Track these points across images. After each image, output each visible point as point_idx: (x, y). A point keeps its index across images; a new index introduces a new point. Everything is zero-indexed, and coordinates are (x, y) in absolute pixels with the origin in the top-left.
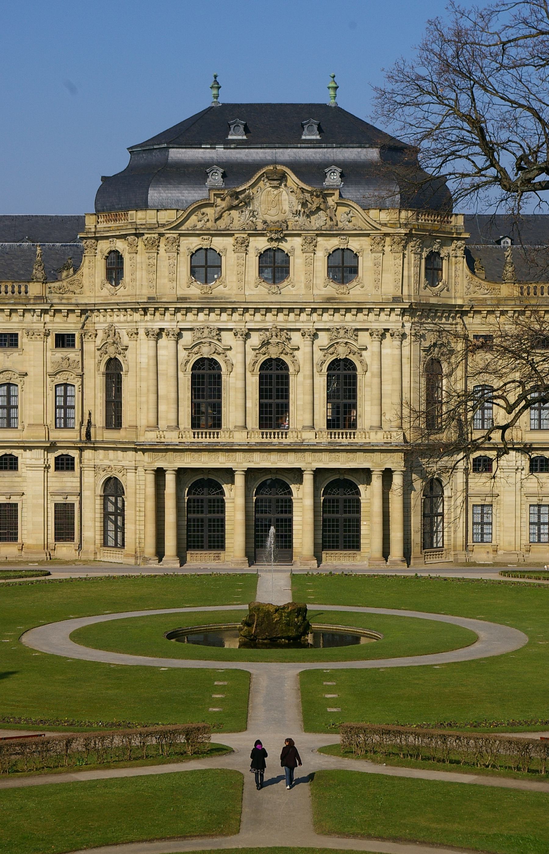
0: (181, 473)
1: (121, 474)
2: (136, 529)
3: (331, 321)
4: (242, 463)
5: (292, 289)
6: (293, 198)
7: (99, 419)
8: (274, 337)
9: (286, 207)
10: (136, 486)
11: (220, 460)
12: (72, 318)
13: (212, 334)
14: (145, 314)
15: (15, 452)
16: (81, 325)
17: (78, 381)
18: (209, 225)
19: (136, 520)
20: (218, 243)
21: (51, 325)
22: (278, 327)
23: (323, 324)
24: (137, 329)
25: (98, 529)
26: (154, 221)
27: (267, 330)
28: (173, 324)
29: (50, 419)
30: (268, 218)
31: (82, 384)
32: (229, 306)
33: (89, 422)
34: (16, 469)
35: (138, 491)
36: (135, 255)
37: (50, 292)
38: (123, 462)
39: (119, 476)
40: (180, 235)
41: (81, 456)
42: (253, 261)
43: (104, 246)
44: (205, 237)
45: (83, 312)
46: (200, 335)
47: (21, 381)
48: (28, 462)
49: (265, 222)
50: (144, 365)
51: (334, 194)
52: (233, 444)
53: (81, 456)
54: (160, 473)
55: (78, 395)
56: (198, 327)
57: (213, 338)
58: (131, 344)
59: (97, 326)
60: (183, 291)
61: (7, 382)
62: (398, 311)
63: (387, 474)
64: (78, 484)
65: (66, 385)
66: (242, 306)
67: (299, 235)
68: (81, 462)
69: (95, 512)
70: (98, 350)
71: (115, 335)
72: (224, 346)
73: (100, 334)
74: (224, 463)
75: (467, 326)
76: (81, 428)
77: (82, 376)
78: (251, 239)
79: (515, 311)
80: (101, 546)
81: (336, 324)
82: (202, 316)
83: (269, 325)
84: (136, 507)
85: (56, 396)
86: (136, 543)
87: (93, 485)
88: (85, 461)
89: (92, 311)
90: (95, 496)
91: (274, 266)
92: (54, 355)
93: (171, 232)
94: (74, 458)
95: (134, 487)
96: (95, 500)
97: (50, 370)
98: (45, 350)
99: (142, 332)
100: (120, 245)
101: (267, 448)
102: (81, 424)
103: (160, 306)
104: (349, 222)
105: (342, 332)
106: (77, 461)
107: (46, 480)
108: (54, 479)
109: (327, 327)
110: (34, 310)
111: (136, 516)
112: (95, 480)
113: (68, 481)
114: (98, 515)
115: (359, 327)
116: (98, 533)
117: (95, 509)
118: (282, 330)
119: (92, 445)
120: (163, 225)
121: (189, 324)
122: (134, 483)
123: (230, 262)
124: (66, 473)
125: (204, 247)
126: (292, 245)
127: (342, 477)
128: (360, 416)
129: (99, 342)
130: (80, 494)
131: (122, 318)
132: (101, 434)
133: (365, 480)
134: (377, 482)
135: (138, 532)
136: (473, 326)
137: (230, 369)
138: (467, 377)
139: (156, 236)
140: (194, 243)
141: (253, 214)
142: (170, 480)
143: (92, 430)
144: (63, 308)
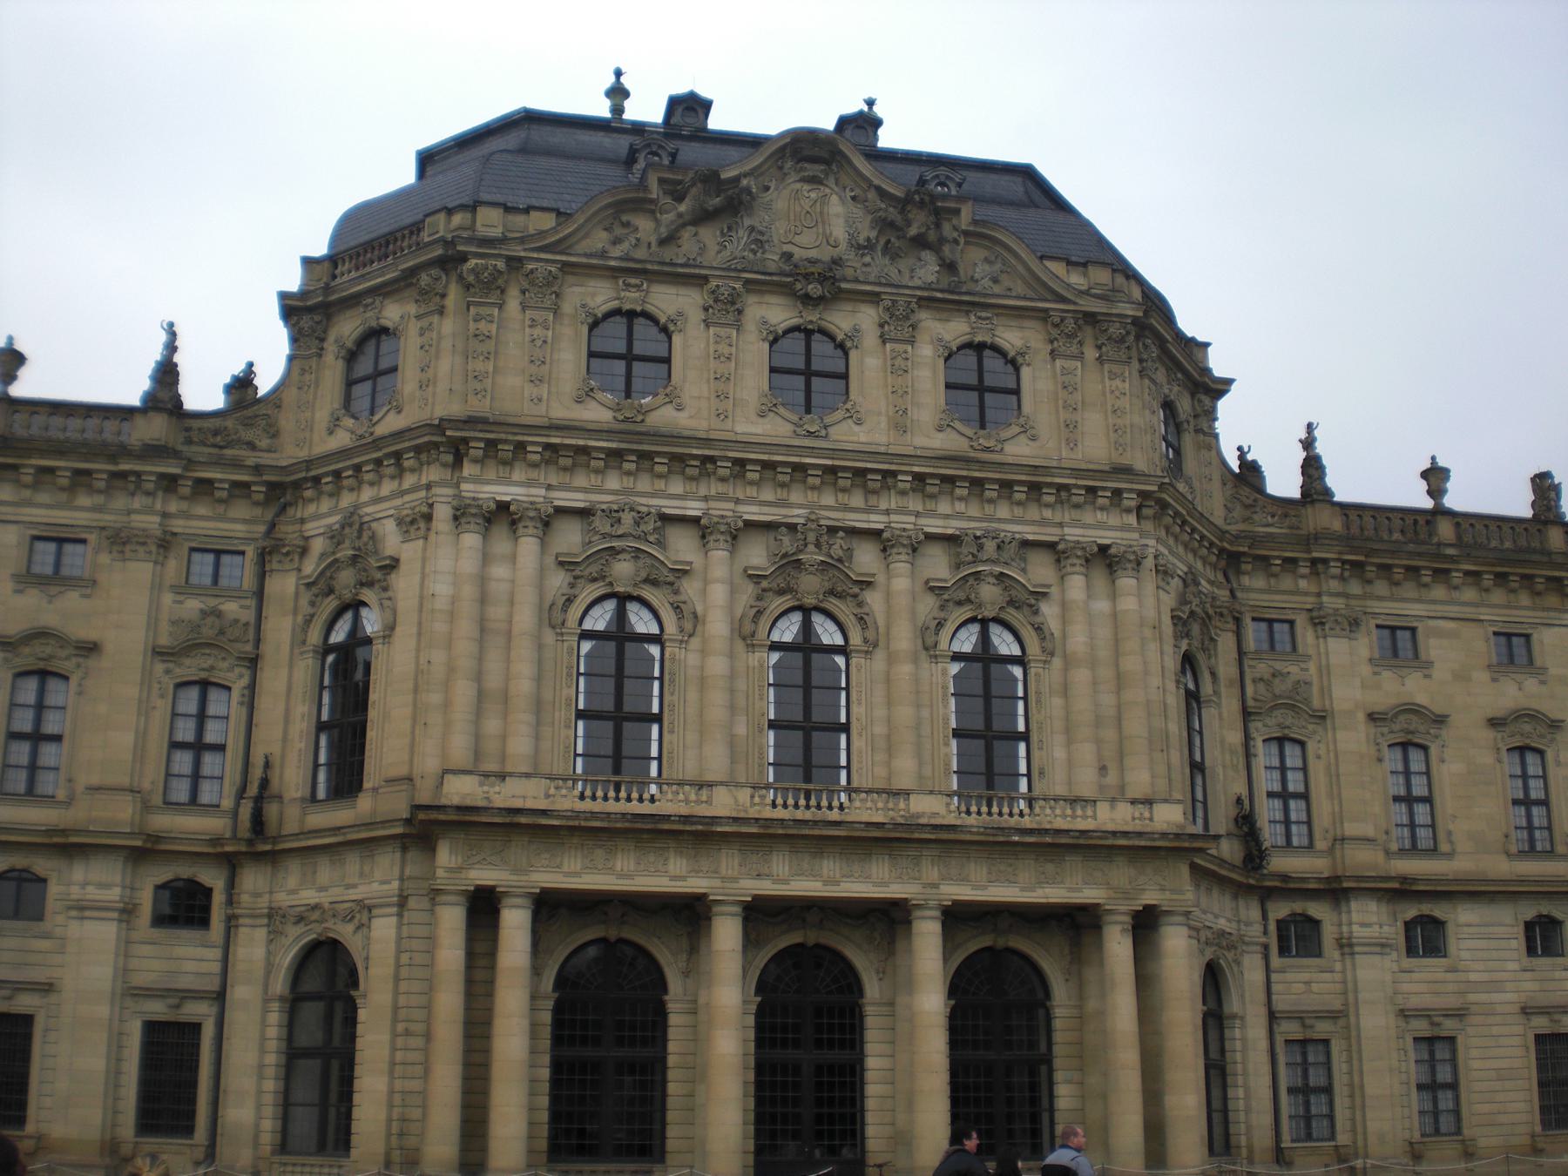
0: (550, 907)
1: (350, 928)
2: (391, 1092)
3: (959, 516)
4: (735, 879)
5: (856, 428)
6: (857, 211)
7: (293, 778)
8: (811, 548)
9: (839, 232)
10: (397, 959)
11: (671, 867)
12: (241, 510)
13: (643, 527)
14: (458, 463)
15: (40, 865)
16: (262, 528)
17: (241, 676)
18: (640, 254)
19: (393, 1064)
20: (666, 300)
21: (181, 522)
22: (823, 522)
23: (940, 522)
24: (431, 506)
25: (269, 1099)
26: (496, 232)
27: (792, 527)
28: (534, 491)
29: (151, 777)
30: (798, 253)
31: (252, 687)
32: (695, 452)
33: (265, 783)
34: (39, 917)
35: (404, 972)
36: (436, 319)
37: (189, 442)
38: (361, 889)
39: (344, 931)
40: (565, 266)
41: (231, 885)
42: (754, 354)
43: (348, 327)
44: (633, 281)
45: (275, 489)
46: (608, 529)
47: (79, 666)
48: (75, 892)
49: (787, 256)
50: (441, 604)
51: (957, 212)
52: (714, 820)
53: (231, 885)
54: (483, 908)
55: (237, 713)
56: (604, 507)
57: (643, 538)
58: (409, 552)
59: (311, 528)
60: (563, 411)
61: (41, 665)
62: (1130, 501)
63: (1145, 924)
64: (216, 967)
65: (205, 685)
66: (731, 454)
67: (873, 298)
68: (230, 901)
69: (263, 1051)
70: (309, 585)
71: (359, 537)
72: (676, 562)
73: (318, 546)
74: (683, 878)
75: (1239, 594)
76: (238, 805)
77: (253, 662)
78: (752, 299)
79: (1344, 562)
80: (273, 1153)
81: (973, 525)
82: (613, 482)
83: (797, 515)
84: (395, 1020)
85: (174, 715)
86: (389, 1135)
87: (259, 963)
88: (245, 898)
89: (297, 485)
90: (266, 1001)
91: (810, 372)
92: (181, 602)
93: (543, 256)
94: (210, 890)
95: (392, 961)
96: (265, 1011)
97: (164, 640)
98: (157, 587)
99: (443, 513)
100: (392, 313)
101: (816, 832)
102: (241, 793)
103: (503, 436)
104: (995, 281)
105: (990, 546)
106: (218, 898)
107: (125, 947)
108: (146, 950)
109: (950, 531)
110: (138, 474)
111: (394, 1049)
112: (269, 952)
113: (189, 957)
114: (271, 1059)
115: (1031, 537)
116: (269, 1111)
117: (263, 1039)
118: (832, 530)
119: (268, 847)
120: (522, 240)
121: (580, 496)
122: (393, 946)
123: (692, 347)
124: (186, 934)
125: (627, 307)
126: (856, 321)
127: (1001, 943)
128: (1041, 773)
129: (310, 567)
130: (220, 997)
131: (387, 487)
132: (293, 816)
133: (1067, 951)
134: (1118, 946)
135: (397, 1099)
136: (1253, 596)
137: (688, 626)
138: (1246, 714)
139: (501, 265)
140: (601, 295)
141: (759, 241)
142: (515, 922)
143: (271, 810)
144: (219, 476)
